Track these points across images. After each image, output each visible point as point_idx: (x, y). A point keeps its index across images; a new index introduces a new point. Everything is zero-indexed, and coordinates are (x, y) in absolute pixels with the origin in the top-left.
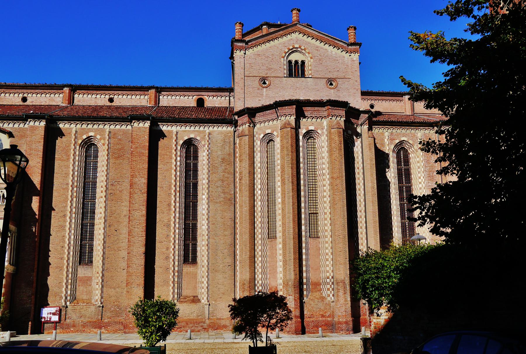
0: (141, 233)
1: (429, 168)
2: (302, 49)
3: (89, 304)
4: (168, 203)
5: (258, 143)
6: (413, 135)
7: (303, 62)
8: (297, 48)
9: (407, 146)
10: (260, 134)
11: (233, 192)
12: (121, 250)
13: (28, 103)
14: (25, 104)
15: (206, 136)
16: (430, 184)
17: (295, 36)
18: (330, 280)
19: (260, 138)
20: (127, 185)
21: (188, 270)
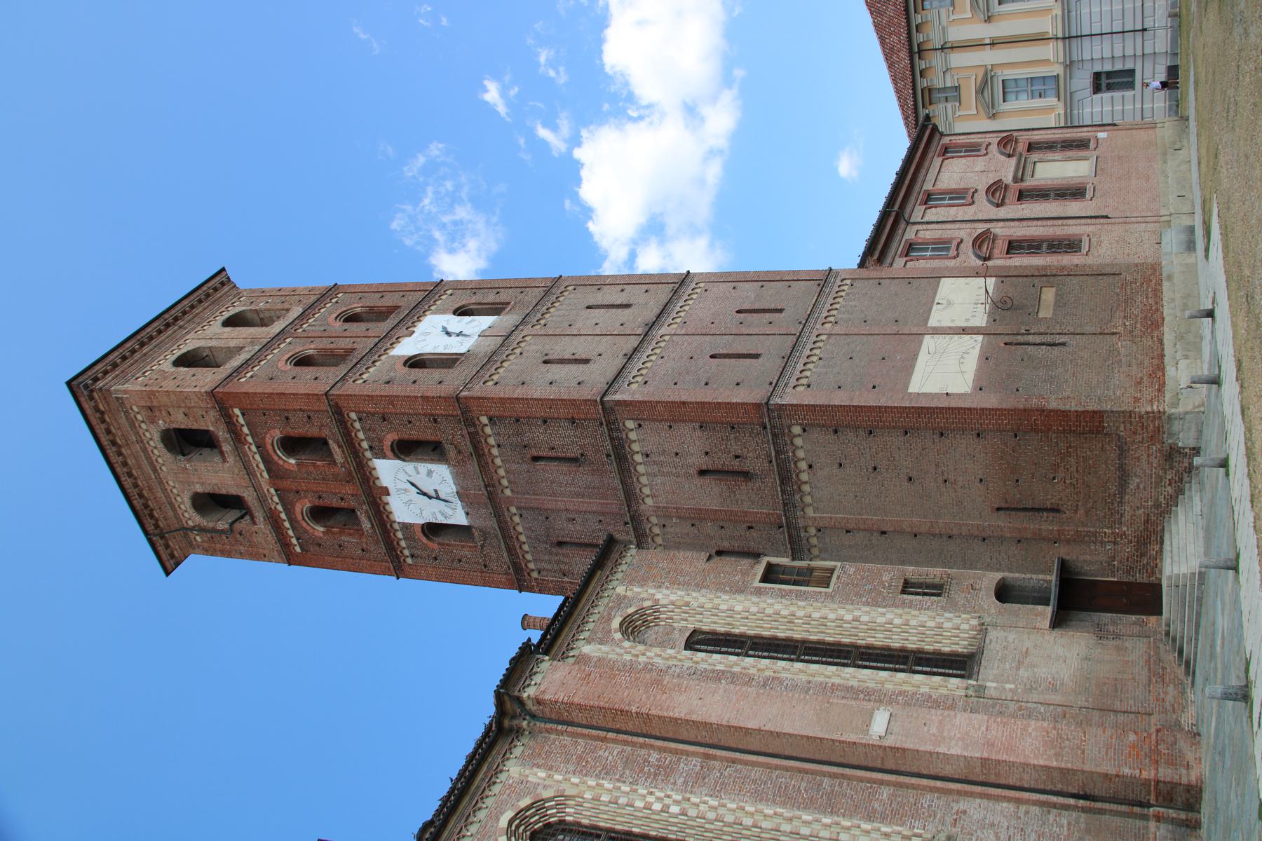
1: (627, 772)
6: (508, 792)
9: (532, 820)
16: (682, 780)
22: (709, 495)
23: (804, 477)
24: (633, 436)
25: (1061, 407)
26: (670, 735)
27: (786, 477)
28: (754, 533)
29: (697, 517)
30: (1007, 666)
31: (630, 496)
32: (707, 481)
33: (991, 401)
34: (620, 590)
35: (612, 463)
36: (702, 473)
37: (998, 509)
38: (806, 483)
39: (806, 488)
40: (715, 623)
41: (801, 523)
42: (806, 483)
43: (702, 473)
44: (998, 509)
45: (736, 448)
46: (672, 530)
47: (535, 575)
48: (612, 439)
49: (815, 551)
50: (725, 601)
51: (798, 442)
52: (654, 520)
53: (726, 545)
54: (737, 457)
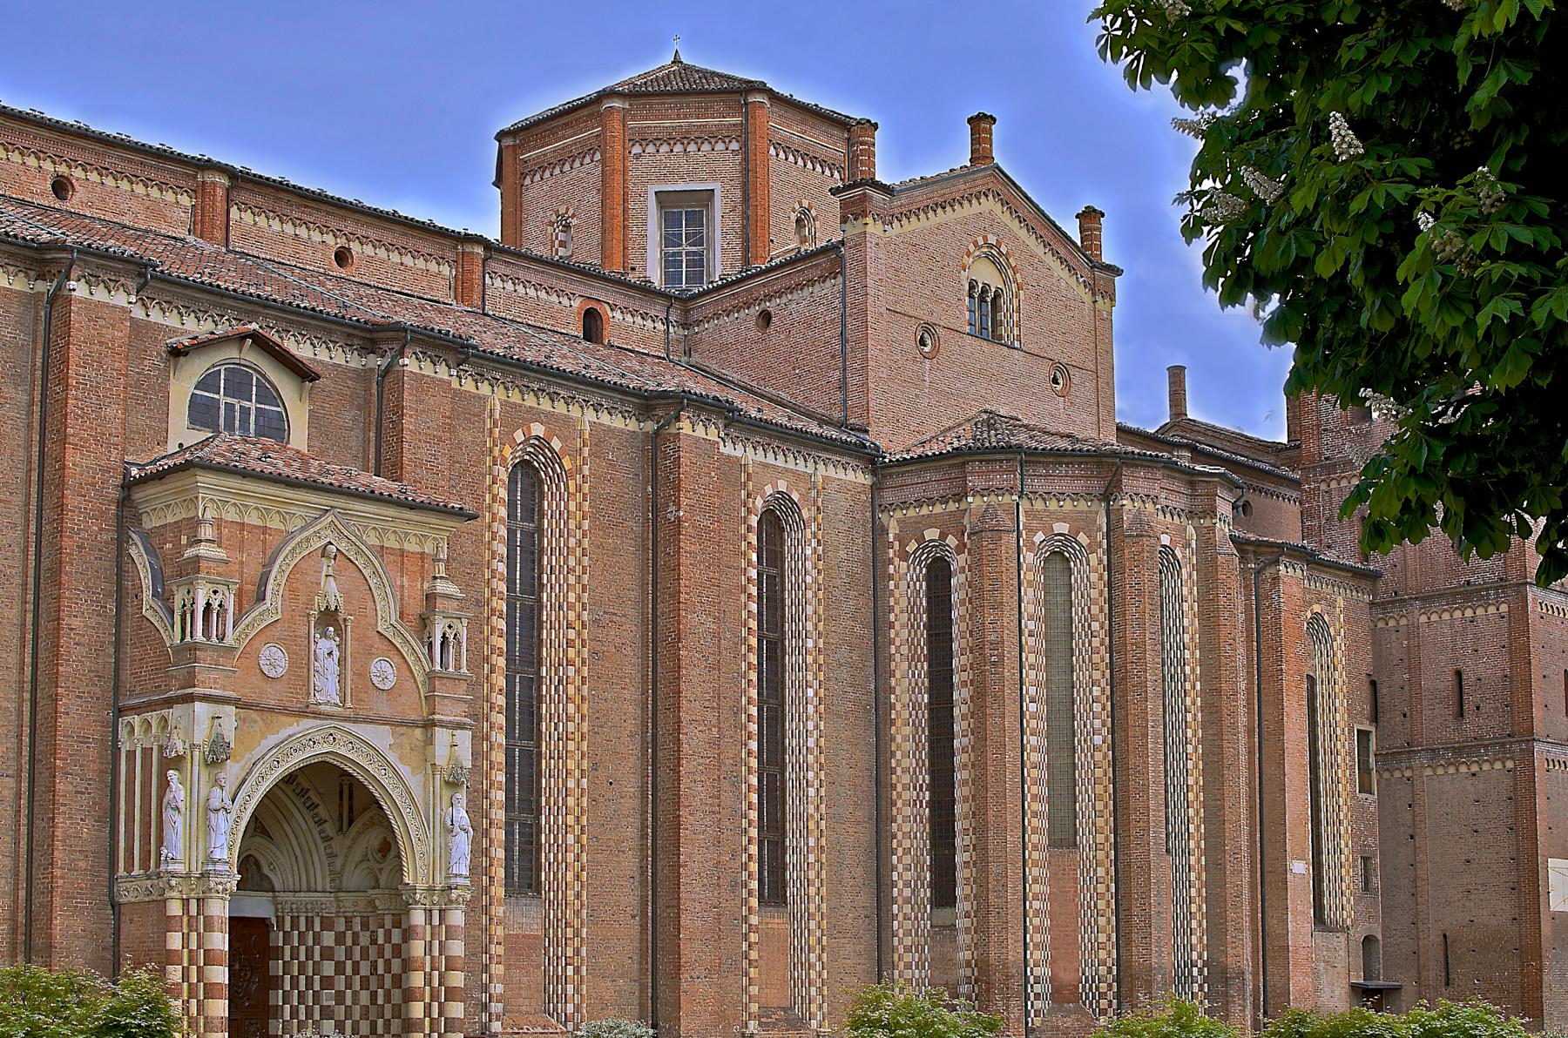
0: (710, 801)
2: (1000, 253)
3: (551, 1031)
4: (732, 704)
5: (1028, 557)
7: (997, 296)
8: (991, 246)
10: (1032, 531)
11: (873, 687)
12: (623, 852)
13: (74, 203)
14: (66, 206)
15: (813, 493)
17: (990, 205)
18: (1201, 972)
19: (1033, 543)
20: (634, 628)
21: (770, 926)
22: (1437, 680)
23: (1463, 769)
24: (1492, 610)
25: (1544, 985)
26: (1264, 698)
27: (1462, 751)
28: (1400, 718)
29: (1412, 664)
30: (1325, 953)
31: (1428, 599)
32: (1450, 678)
33: (1546, 928)
34: (1341, 602)
35: (1461, 586)
36: (1459, 674)
37: (1445, 936)
38: (1457, 770)
39: (1452, 770)
40: (1323, 697)
41: (1416, 763)
42: (1457, 770)
43: (1459, 674)
44: (1445, 936)
45: (1487, 707)
46: (1394, 639)
47: (1323, 487)
48: (1487, 589)
49: (1386, 775)
50: (1341, 703)
51: (1498, 765)
52: (1403, 622)
53: (1383, 690)
54: (1478, 708)
